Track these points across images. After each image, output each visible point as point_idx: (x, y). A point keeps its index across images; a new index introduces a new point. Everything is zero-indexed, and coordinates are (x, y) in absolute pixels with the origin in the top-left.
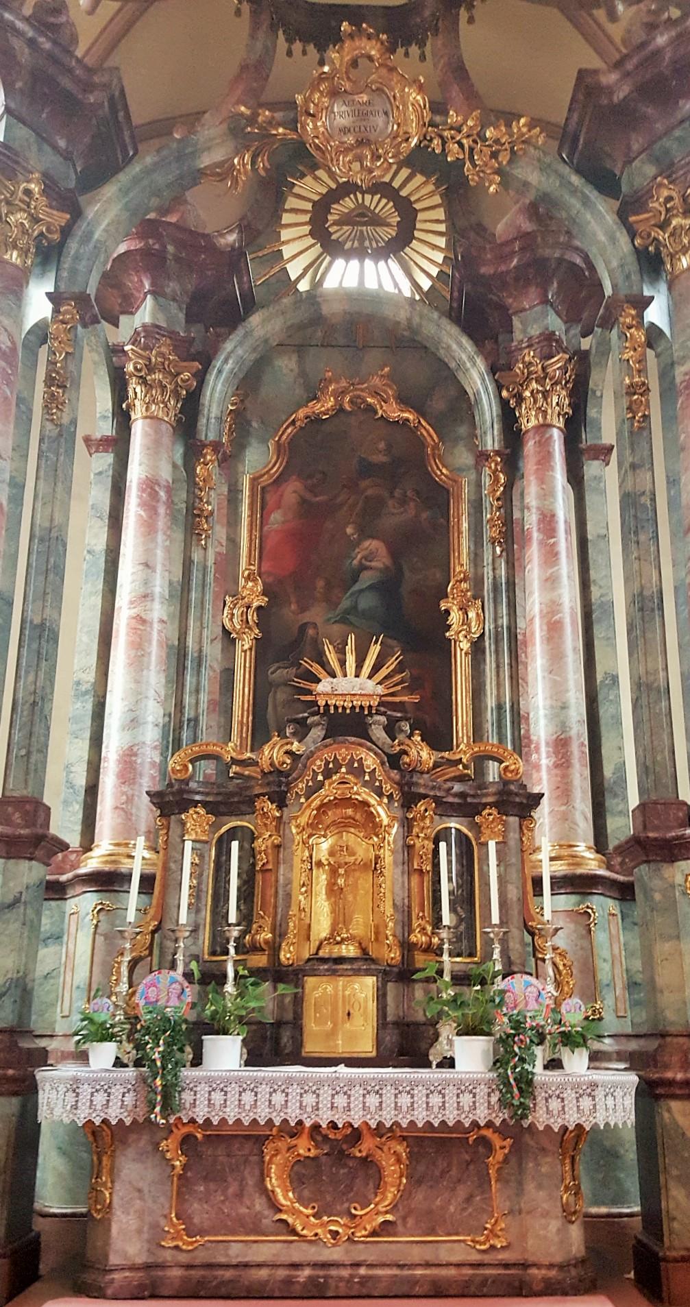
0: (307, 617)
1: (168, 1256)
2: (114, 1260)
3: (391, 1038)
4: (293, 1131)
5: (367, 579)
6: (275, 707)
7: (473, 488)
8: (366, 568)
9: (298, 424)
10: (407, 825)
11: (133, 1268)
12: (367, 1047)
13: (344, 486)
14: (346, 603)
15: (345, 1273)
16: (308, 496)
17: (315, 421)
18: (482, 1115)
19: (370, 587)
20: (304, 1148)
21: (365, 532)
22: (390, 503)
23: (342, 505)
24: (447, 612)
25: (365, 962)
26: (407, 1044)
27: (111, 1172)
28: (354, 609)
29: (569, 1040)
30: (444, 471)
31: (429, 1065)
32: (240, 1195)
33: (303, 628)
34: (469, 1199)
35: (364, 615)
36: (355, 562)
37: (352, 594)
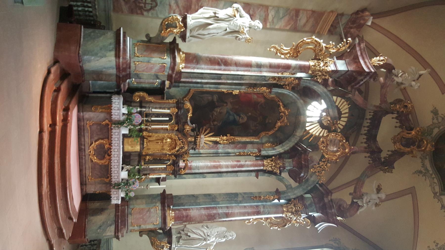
0: (229, 105)
1: (85, 121)
2: (85, 113)
3: (127, 154)
4: (110, 144)
5: (237, 118)
11: (83, 116)
12: (126, 150)
14: (231, 113)
15: (84, 154)
17: (279, 106)
18: (113, 180)
19: (235, 118)
20: (107, 146)
26: (127, 158)
27: (102, 112)
28: (230, 114)
31: (122, 164)
32: (98, 135)
33: (226, 103)
34: (98, 175)
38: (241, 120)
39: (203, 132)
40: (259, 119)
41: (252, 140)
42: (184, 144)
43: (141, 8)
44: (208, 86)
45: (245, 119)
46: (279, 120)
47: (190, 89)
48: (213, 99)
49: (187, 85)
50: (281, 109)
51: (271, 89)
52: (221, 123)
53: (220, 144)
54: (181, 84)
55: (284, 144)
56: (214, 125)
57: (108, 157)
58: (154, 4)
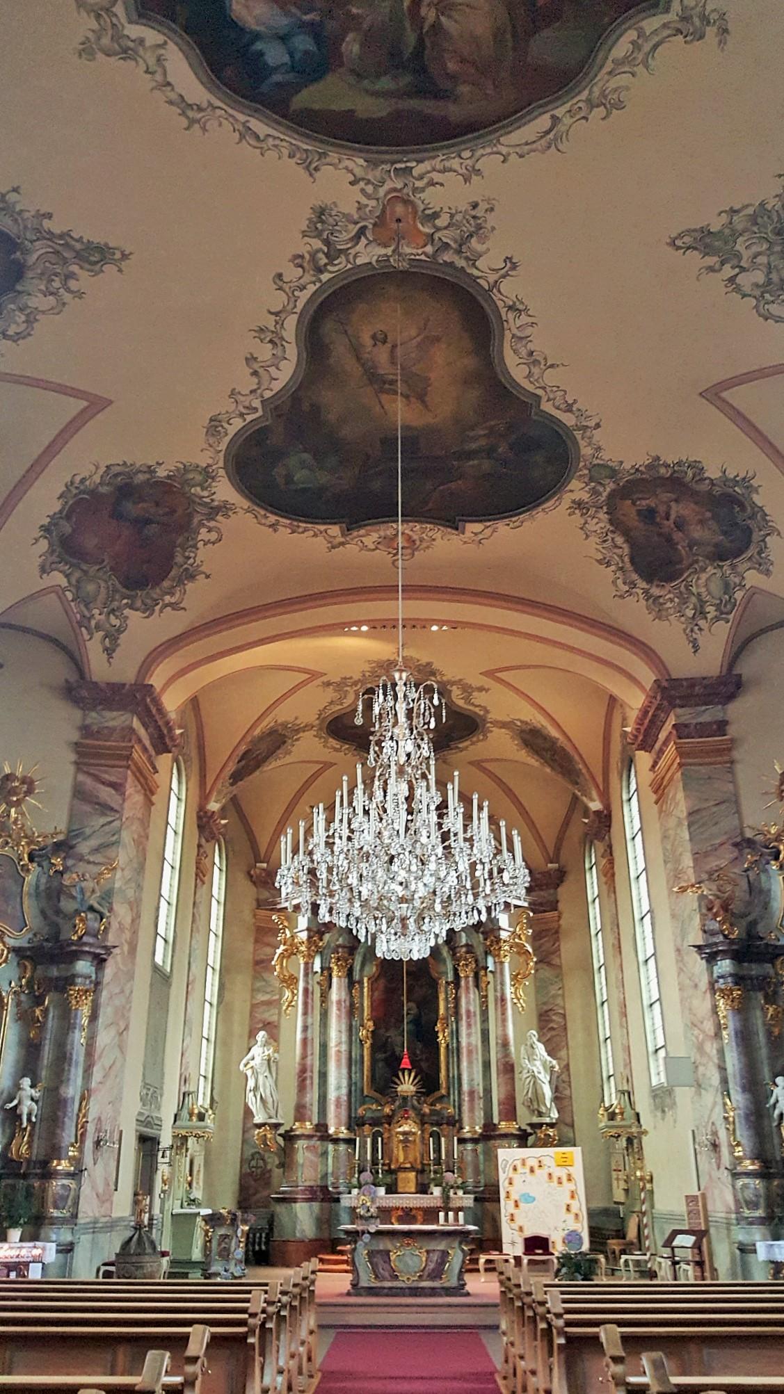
4: (397, 1209)
10: (423, 1132)
12: (413, 1190)
25: (412, 1169)
29: (458, 1187)
43: (263, 1174)
56: (422, 1052)
57: (414, 1212)
58: (257, 1156)
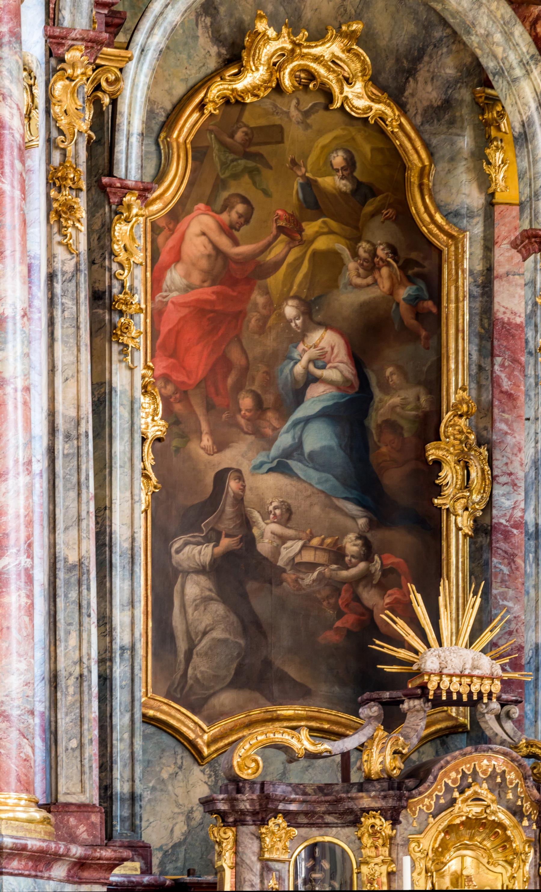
0: (228, 459)
5: (318, 397)
6: (183, 606)
7: (479, 252)
8: (316, 380)
9: (210, 108)
13: (281, 230)
14: (285, 440)
16: (224, 243)
17: (233, 103)
19: (325, 414)
21: (314, 311)
22: (352, 265)
23: (277, 265)
24: (438, 464)
28: (296, 450)
30: (438, 217)
33: (221, 477)
35: (313, 460)
36: (299, 369)
37: (295, 424)
38: (330, 374)
39: (403, 654)
40: (322, 244)
41: (466, 283)
42: (475, 773)
44: (120, 617)
45: (324, 339)
46: (329, 96)
47: (147, 720)
48: (201, 570)
49: (120, 748)
50: (253, 91)
51: (126, 189)
52: (352, 508)
53: (489, 505)
54: (121, 787)
55: (489, 64)
56: (368, 552)
